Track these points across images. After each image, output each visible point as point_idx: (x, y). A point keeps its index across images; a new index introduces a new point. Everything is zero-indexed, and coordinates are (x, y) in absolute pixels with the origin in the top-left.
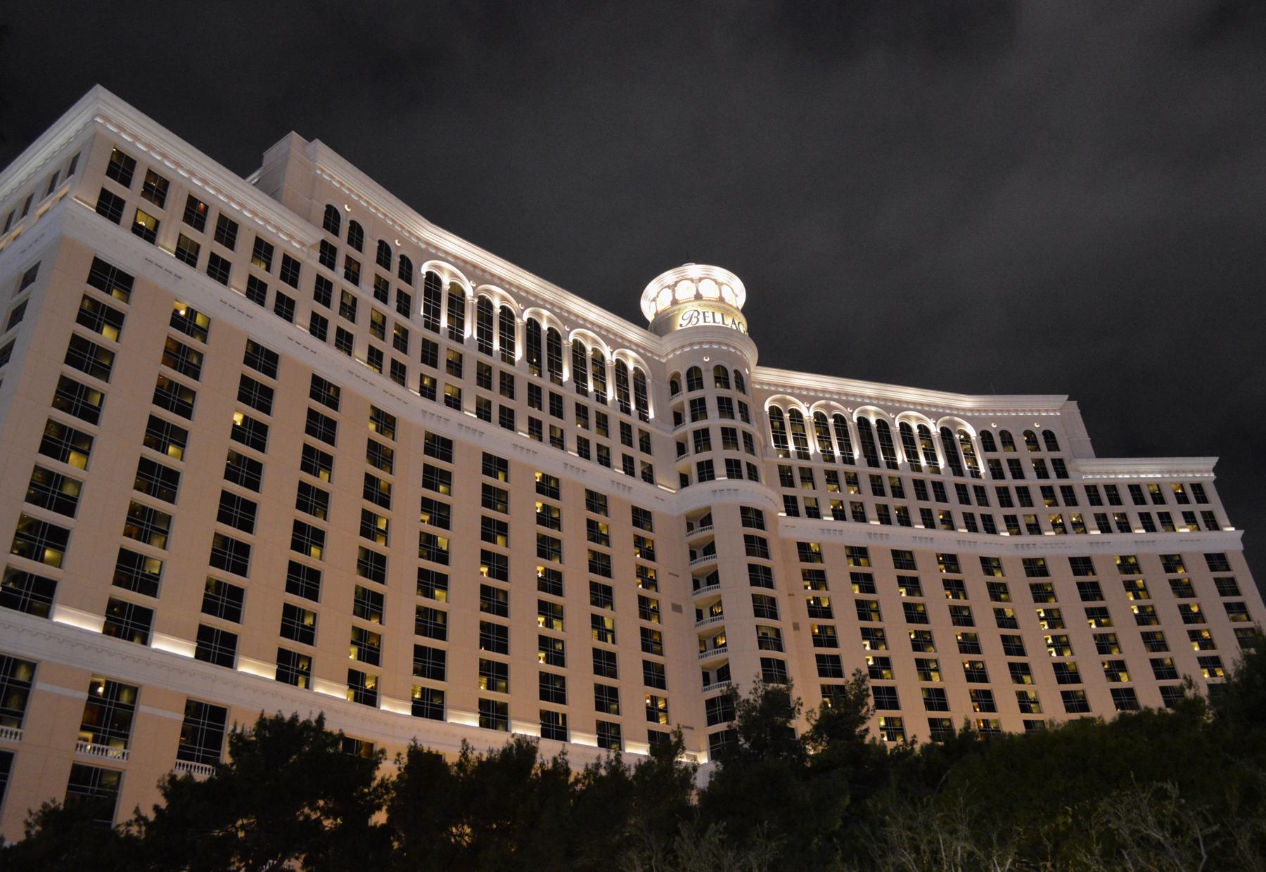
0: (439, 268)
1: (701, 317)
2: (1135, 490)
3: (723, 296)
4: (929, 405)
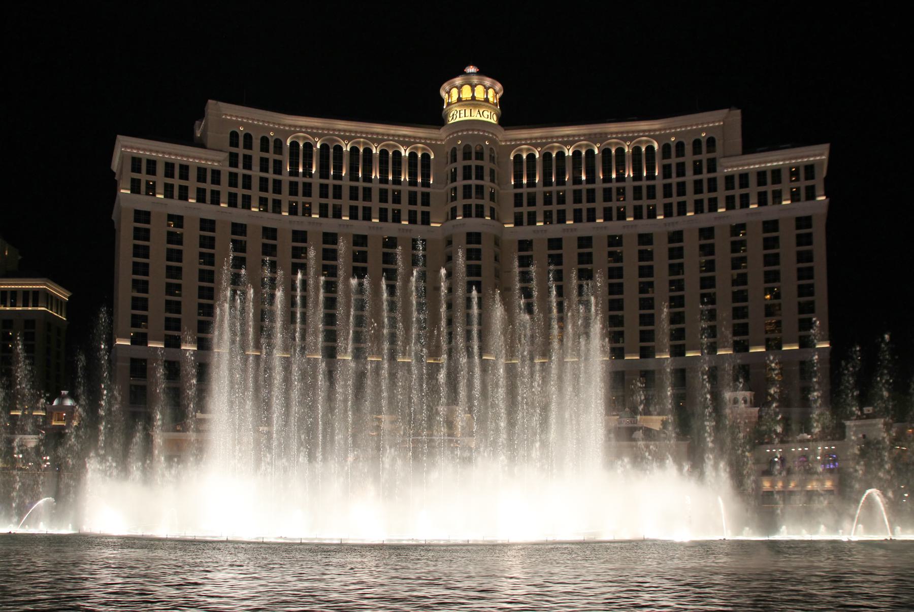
0: (298, 137)
1: (458, 115)
2: (761, 176)
3: (475, 95)
4: (622, 133)
